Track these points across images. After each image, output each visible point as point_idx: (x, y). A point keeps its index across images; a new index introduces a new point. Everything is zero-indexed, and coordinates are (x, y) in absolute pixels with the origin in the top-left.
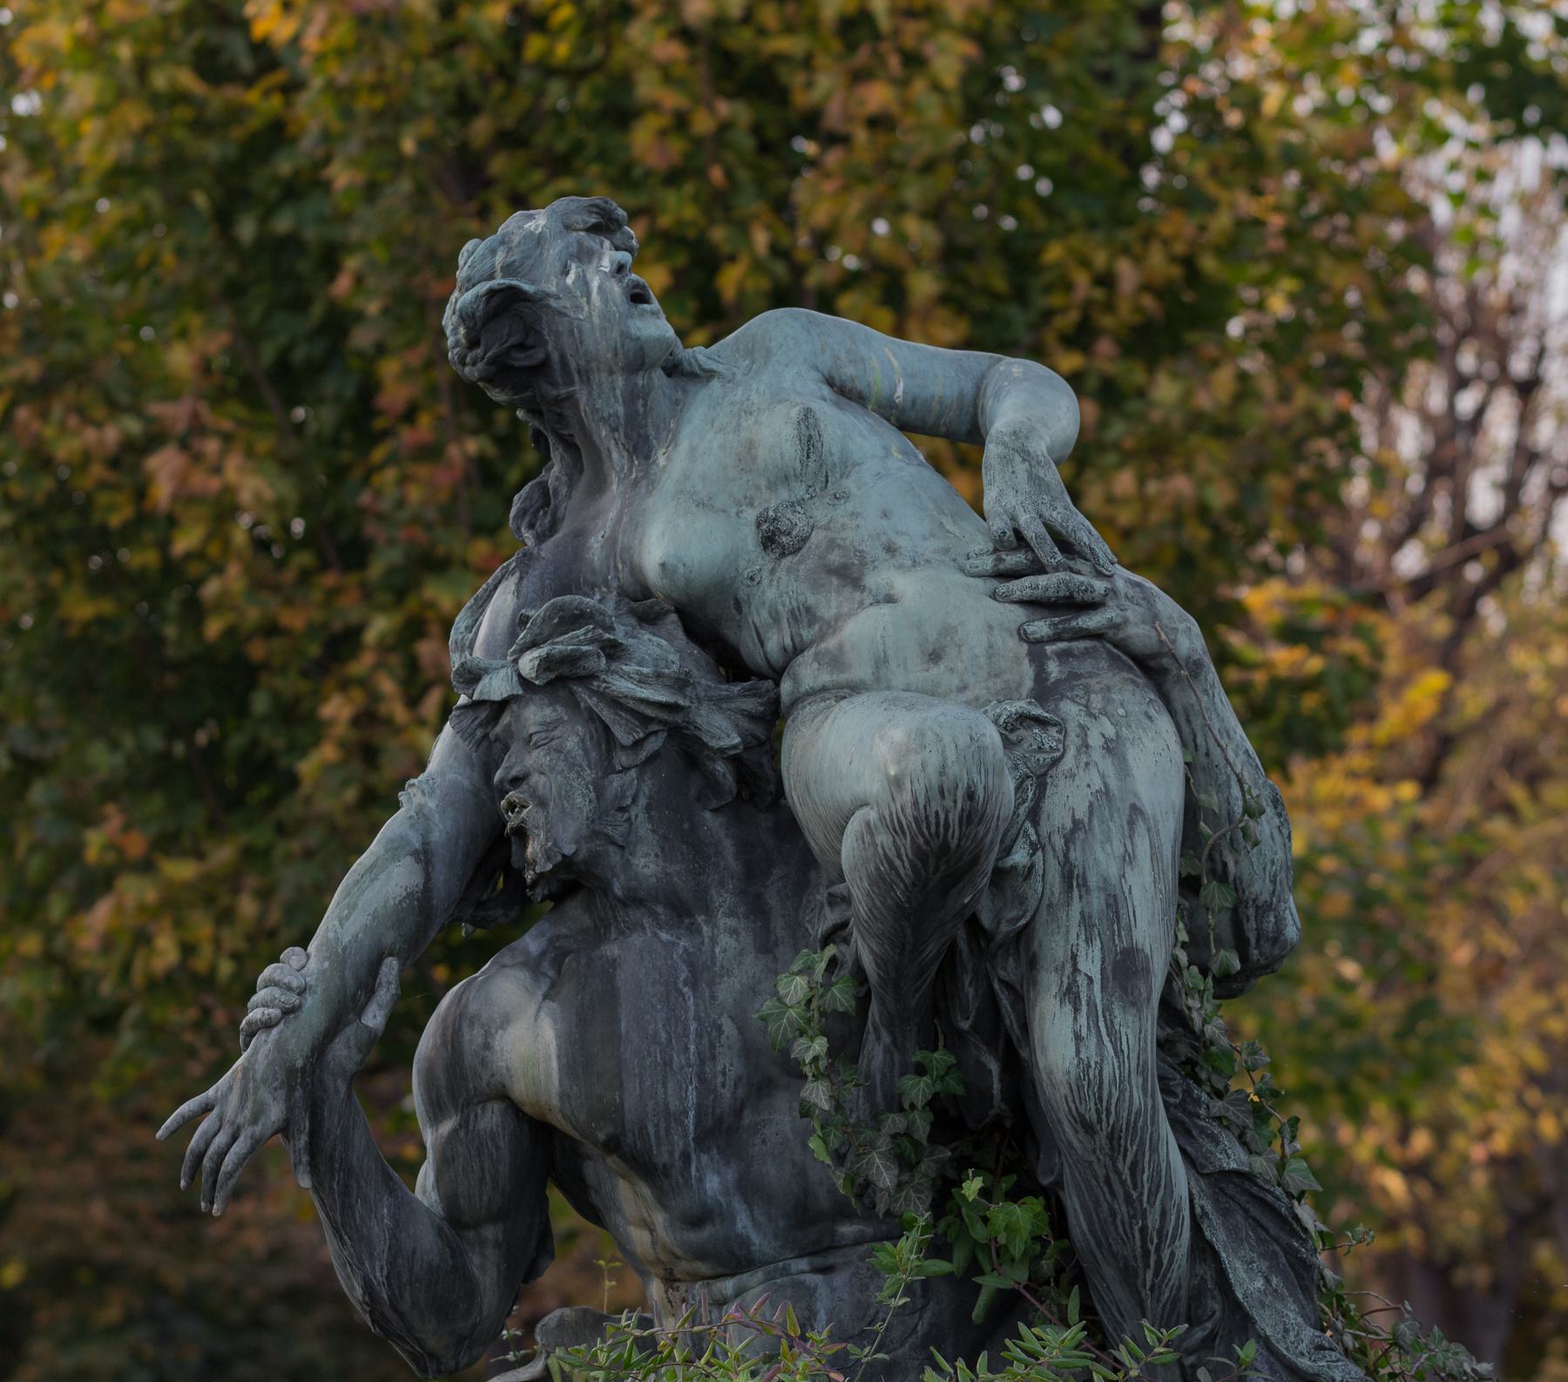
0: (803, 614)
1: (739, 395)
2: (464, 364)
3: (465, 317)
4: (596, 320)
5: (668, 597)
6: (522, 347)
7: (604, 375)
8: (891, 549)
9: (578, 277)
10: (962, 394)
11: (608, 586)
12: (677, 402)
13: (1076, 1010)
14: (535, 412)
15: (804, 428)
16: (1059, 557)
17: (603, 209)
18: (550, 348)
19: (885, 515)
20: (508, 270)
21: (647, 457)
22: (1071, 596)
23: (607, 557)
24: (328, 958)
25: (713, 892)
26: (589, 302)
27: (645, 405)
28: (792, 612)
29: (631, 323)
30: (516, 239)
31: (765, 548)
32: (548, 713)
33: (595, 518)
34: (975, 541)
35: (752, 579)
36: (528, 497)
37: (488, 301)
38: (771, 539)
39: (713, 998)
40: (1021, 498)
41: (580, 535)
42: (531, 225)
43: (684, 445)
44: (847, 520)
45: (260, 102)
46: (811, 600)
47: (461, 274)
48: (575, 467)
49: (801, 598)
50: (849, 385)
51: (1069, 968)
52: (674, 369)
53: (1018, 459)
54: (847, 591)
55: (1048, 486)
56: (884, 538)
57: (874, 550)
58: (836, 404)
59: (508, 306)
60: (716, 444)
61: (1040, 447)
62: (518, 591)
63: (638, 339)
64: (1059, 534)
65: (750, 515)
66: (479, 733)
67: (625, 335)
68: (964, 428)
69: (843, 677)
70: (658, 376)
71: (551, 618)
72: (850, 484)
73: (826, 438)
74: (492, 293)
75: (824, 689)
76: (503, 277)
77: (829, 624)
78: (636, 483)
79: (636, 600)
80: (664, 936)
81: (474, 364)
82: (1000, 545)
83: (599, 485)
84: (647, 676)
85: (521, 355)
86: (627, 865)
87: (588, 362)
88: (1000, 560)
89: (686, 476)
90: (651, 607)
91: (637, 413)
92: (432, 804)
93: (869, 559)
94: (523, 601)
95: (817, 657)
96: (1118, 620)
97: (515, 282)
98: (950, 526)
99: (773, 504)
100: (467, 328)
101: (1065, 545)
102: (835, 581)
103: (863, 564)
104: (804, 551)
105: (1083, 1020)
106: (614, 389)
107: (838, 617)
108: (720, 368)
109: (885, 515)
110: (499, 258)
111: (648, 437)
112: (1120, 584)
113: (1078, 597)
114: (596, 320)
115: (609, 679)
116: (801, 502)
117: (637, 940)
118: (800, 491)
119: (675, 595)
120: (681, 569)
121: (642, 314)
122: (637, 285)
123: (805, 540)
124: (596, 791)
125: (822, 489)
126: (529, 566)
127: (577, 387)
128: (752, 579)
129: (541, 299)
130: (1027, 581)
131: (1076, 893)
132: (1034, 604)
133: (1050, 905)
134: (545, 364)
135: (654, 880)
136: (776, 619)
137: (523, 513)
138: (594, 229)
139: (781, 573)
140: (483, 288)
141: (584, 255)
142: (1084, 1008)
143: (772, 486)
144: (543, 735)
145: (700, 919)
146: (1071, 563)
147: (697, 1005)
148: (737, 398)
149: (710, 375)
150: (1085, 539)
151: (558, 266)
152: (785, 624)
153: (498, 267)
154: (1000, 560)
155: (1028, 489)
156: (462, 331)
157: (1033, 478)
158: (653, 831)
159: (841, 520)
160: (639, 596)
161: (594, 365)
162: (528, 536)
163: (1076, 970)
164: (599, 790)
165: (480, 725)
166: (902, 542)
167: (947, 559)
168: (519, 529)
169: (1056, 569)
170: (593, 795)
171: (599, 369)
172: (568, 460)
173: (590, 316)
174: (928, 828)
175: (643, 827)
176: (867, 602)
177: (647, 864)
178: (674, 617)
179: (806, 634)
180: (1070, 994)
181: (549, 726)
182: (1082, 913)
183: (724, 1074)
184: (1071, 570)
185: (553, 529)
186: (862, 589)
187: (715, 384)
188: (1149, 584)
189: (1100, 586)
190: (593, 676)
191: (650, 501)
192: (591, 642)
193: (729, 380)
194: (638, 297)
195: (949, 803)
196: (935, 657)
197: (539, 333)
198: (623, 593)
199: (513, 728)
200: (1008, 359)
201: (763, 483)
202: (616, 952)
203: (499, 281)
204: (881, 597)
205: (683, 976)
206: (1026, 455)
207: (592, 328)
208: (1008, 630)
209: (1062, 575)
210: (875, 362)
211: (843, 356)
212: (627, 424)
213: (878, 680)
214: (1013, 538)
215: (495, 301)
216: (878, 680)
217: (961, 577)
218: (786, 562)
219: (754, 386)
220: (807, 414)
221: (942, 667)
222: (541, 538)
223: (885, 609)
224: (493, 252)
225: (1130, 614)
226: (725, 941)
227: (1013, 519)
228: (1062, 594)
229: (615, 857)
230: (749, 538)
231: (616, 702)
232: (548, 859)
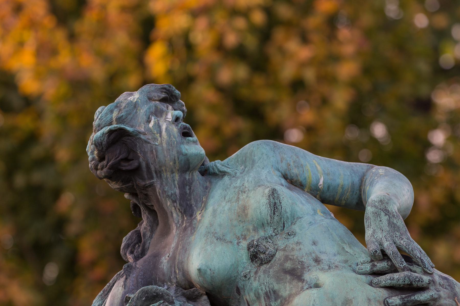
0: (272, 295)
1: (238, 183)
2: (97, 169)
3: (97, 144)
4: (164, 145)
5: (202, 287)
6: (126, 160)
7: (169, 174)
8: (317, 261)
9: (155, 123)
10: (353, 184)
11: (171, 282)
12: (206, 188)
14: (134, 194)
15: (272, 199)
16: (405, 264)
17: (168, 90)
18: (141, 160)
19: (314, 243)
20: (120, 120)
21: (191, 215)
22: (411, 284)
23: (171, 267)
26: (161, 136)
27: (190, 189)
28: (266, 293)
29: (182, 146)
30: (123, 105)
31: (252, 261)
33: (164, 247)
34: (361, 256)
35: (245, 277)
36: (130, 238)
37: (109, 136)
38: (256, 256)
40: (385, 234)
41: (157, 256)
42: (131, 98)
43: (210, 209)
44: (294, 246)
45: (25, 122)
46: (276, 287)
47: (95, 123)
48: (154, 223)
49: (271, 286)
50: (295, 179)
52: (205, 172)
53: (383, 214)
54: (295, 282)
55: (399, 228)
56: (314, 255)
57: (308, 261)
58: (289, 188)
59: (120, 139)
60: (226, 208)
61: (394, 208)
62: (125, 285)
63: (186, 155)
64: (405, 252)
65: (244, 244)
67: (180, 153)
68: (355, 202)
70: (197, 175)
72: (296, 228)
73: (283, 204)
74: (111, 132)
76: (117, 124)
77: (285, 299)
78: (185, 229)
79: (185, 289)
81: (102, 169)
82: (374, 258)
83: (166, 231)
85: (127, 164)
87: (160, 167)
88: (374, 266)
89: (211, 225)
90: (194, 292)
91: (186, 193)
93: (306, 265)
94: (127, 290)
96: (436, 296)
97: (123, 126)
98: (348, 249)
99: (256, 238)
100: (98, 150)
101: (408, 259)
102: (288, 277)
103: (303, 268)
106: (174, 181)
108: (228, 170)
109: (314, 243)
110: (115, 115)
111: (191, 205)
112: (437, 278)
113: (415, 284)
114: (164, 145)
116: (271, 237)
118: (270, 231)
119: (206, 285)
120: (209, 272)
121: (188, 142)
122: (185, 128)
123: (273, 256)
125: (281, 230)
126: (130, 272)
127: (155, 180)
128: (245, 277)
129: (136, 135)
130: (388, 276)
132: (391, 288)
134: (138, 169)
136: (258, 297)
137: (127, 246)
138: (163, 100)
139: (261, 273)
140: (106, 129)
141: (158, 113)
143: (255, 229)
146: (411, 267)
148: (238, 185)
149: (224, 174)
150: (418, 255)
151: (145, 118)
153: (114, 119)
154: (374, 266)
155: (388, 229)
156: (96, 152)
157: (391, 224)
159: (292, 246)
160: (188, 287)
161: (163, 168)
162: (130, 258)
166: (323, 257)
167: (346, 265)
168: (125, 254)
169: (403, 270)
171: (166, 170)
172: (151, 219)
173: (161, 143)
176: (305, 287)
178: (205, 297)
184: (411, 270)
185: (143, 253)
186: (303, 281)
187: (226, 178)
188: (451, 278)
189: (426, 279)
193: (233, 176)
194: (186, 134)
197: (135, 152)
198: (178, 285)
200: (377, 167)
201: (251, 227)
203: (115, 126)
204: (312, 285)
206: (387, 212)
207: (163, 149)
208: (378, 301)
209: (406, 273)
210: (308, 167)
211: (292, 164)
212: (181, 199)
214: (380, 254)
215: (112, 137)
217: (354, 275)
218: (263, 268)
219: (246, 179)
220: (273, 192)
222: (136, 259)
223: (314, 291)
224: (112, 111)
225: (442, 293)
227: (381, 244)
228: (406, 282)
230: (244, 256)
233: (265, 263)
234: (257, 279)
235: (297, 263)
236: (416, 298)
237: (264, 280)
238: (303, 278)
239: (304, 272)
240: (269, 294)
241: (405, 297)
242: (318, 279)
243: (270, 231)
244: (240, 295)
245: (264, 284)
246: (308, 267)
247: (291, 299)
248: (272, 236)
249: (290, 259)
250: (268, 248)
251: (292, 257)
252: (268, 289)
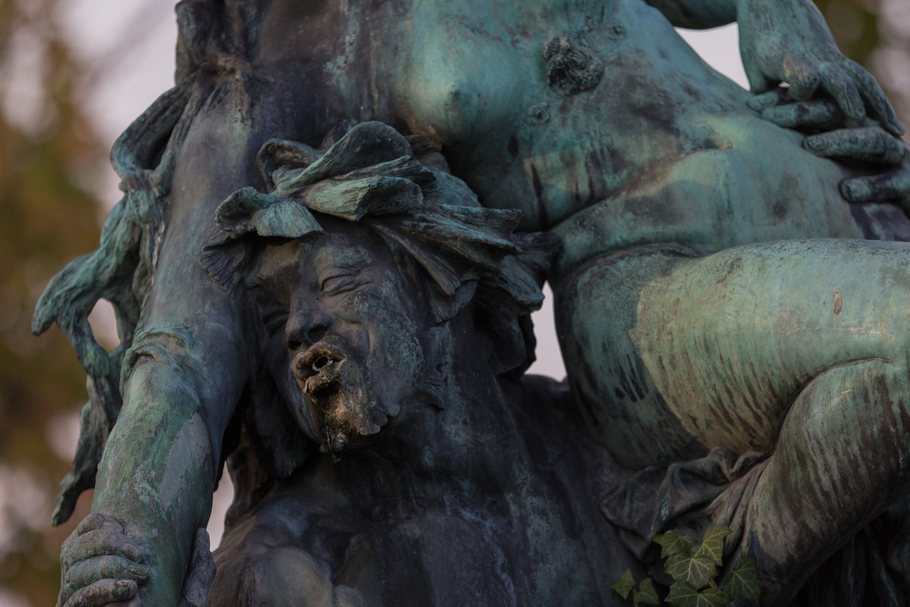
0: (606, 159)
23: (359, 85)
24: (153, 525)
25: (515, 467)
28: (593, 156)
32: (350, 255)
35: (540, 116)
38: (565, 74)
39: (534, 587)
46: (618, 142)
49: (606, 140)
54: (660, 134)
66: (236, 278)
69: (671, 229)
71: (355, 146)
75: (643, 242)
77: (641, 170)
80: (467, 515)
84: (475, 216)
86: (440, 432)
92: (196, 356)
95: (630, 205)
102: (644, 123)
104: (600, 87)
107: (653, 163)
115: (430, 217)
117: (439, 519)
120: (475, 100)
124: (422, 344)
128: (540, 116)
135: (464, 450)
136: (569, 163)
144: (347, 279)
145: (509, 496)
147: (518, 594)
152: (581, 170)
158: (463, 395)
164: (425, 343)
165: (238, 268)
170: (419, 348)
175: (453, 392)
177: (457, 432)
179: (611, 180)
181: (352, 269)
186: (677, 133)
190: (406, 214)
191: (405, 25)
192: (405, 174)
196: (779, 210)
199: (301, 270)
201: (537, 10)
202: (418, 532)
213: (719, 233)
216: (719, 233)
218: (580, 99)
221: (789, 222)
226: (536, 522)
229: (430, 423)
231: (435, 245)
232: (374, 420)
233: (586, 90)
234: (570, 122)
235: (656, 94)
236: (894, 184)
237: (587, 127)
238: (675, 126)
239: (675, 114)
240: (599, 156)
241: (876, 182)
242: (712, 131)
243: (580, 22)
244: (515, 156)
245: (588, 134)
246: (680, 103)
247: (658, 170)
248: (583, 32)
249: (641, 84)
250: (591, 58)
251: (642, 81)
252: (597, 146)
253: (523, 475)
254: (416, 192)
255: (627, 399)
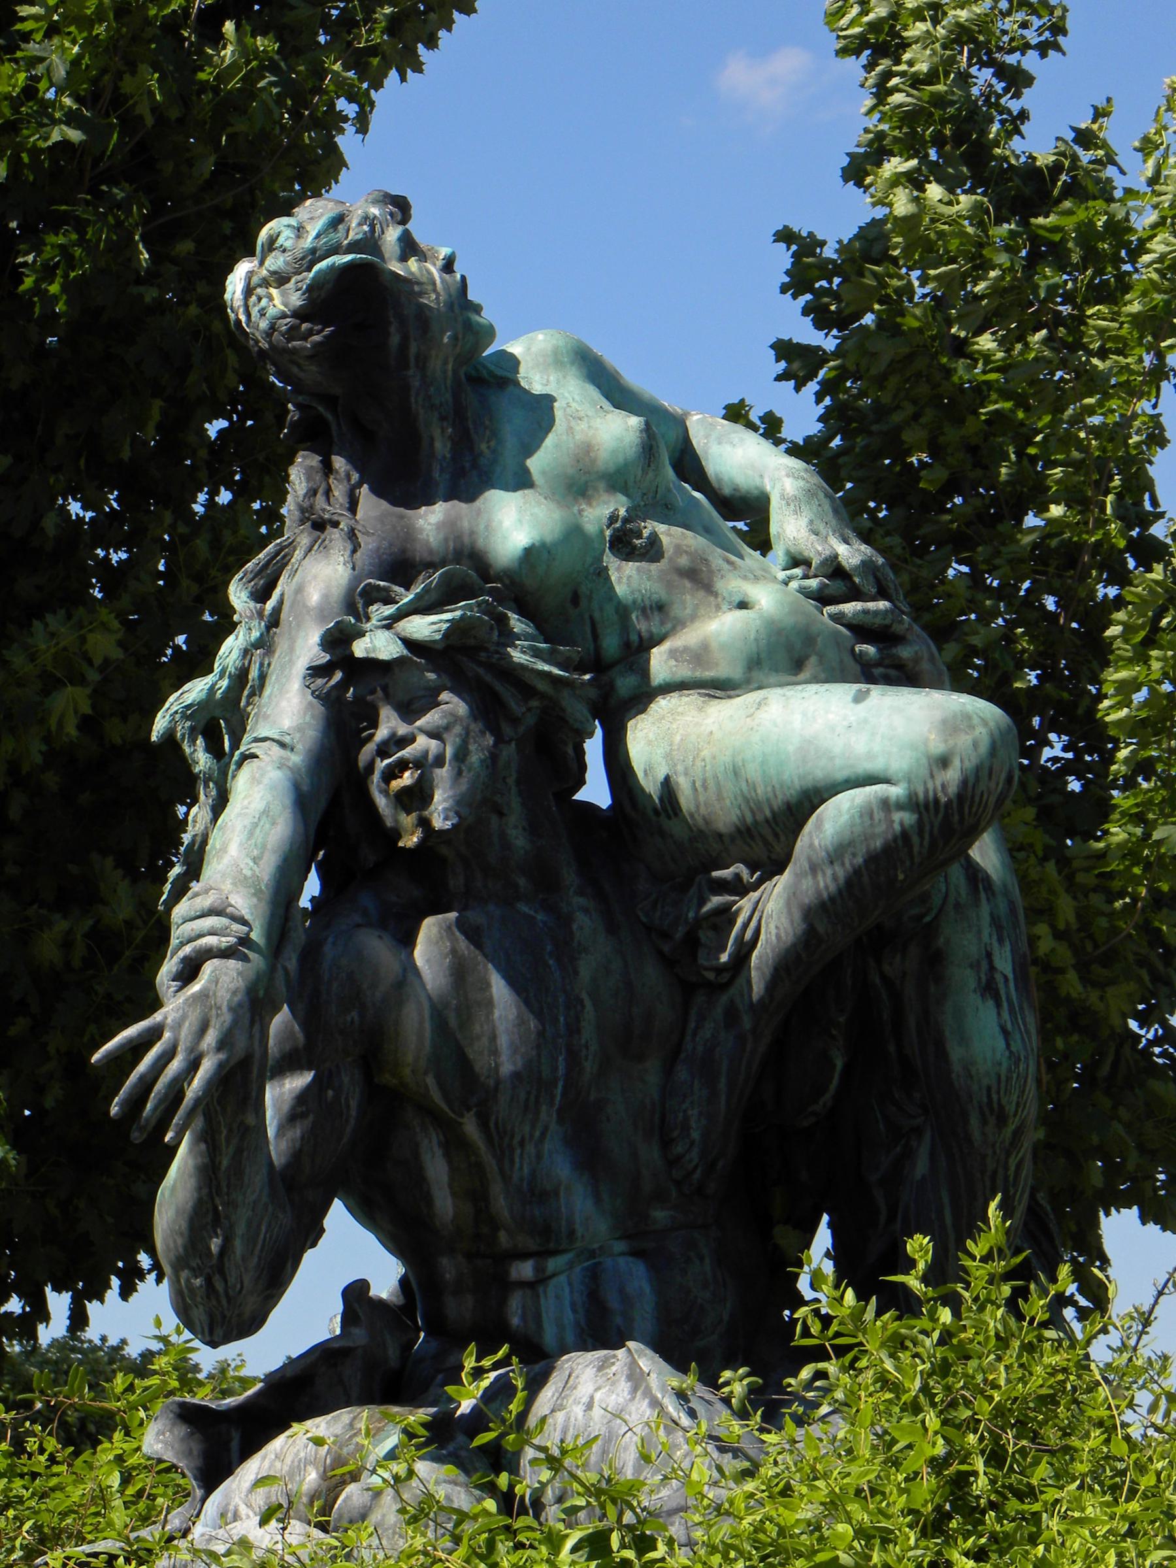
13: (998, 1005)
39: (576, 973)
51: (984, 965)
54: (701, 594)
69: (709, 674)
102: (688, 584)
105: (1006, 1015)
131: (983, 895)
133: (957, 905)
142: (1005, 1005)
163: (992, 968)
174: (970, 807)
175: (515, 802)
180: (989, 989)
182: (992, 914)
183: (587, 1048)
186: (716, 595)
190: (481, 648)
195: (992, 785)
205: (549, 948)
253: (570, 877)
254: (492, 628)
255: (663, 817)
